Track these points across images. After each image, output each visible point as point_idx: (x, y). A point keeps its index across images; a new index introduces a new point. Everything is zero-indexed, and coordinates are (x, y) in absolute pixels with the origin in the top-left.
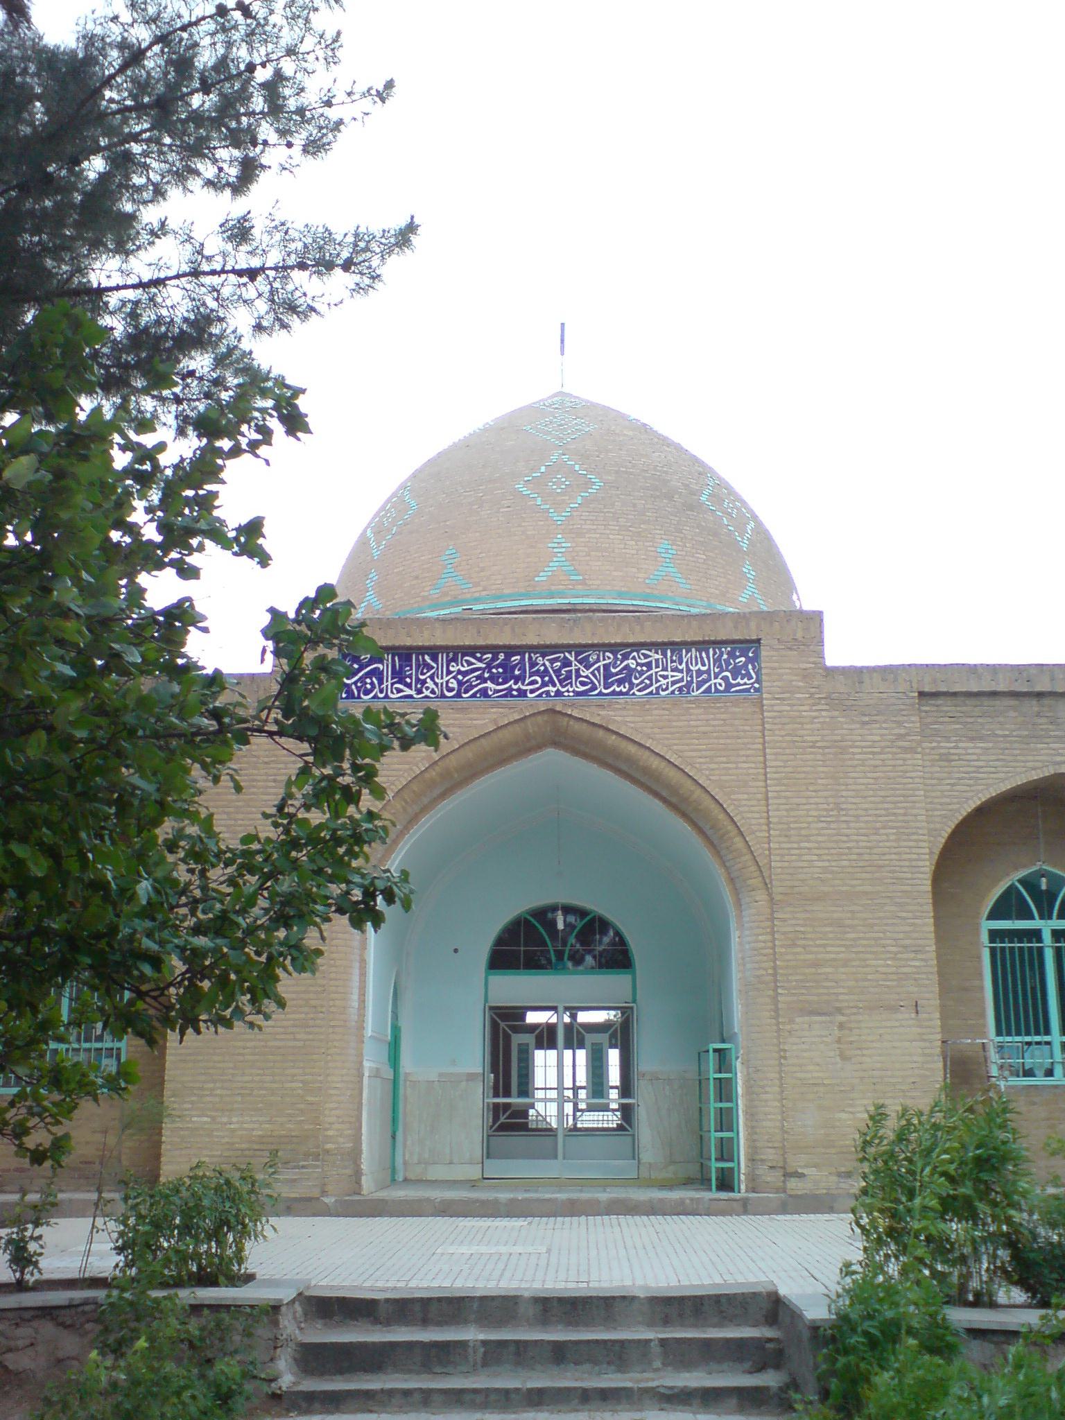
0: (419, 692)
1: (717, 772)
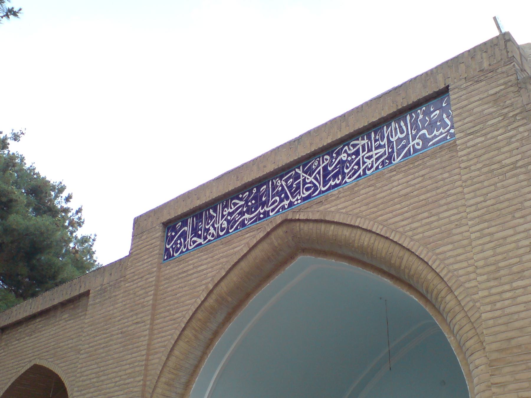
1: (420, 230)
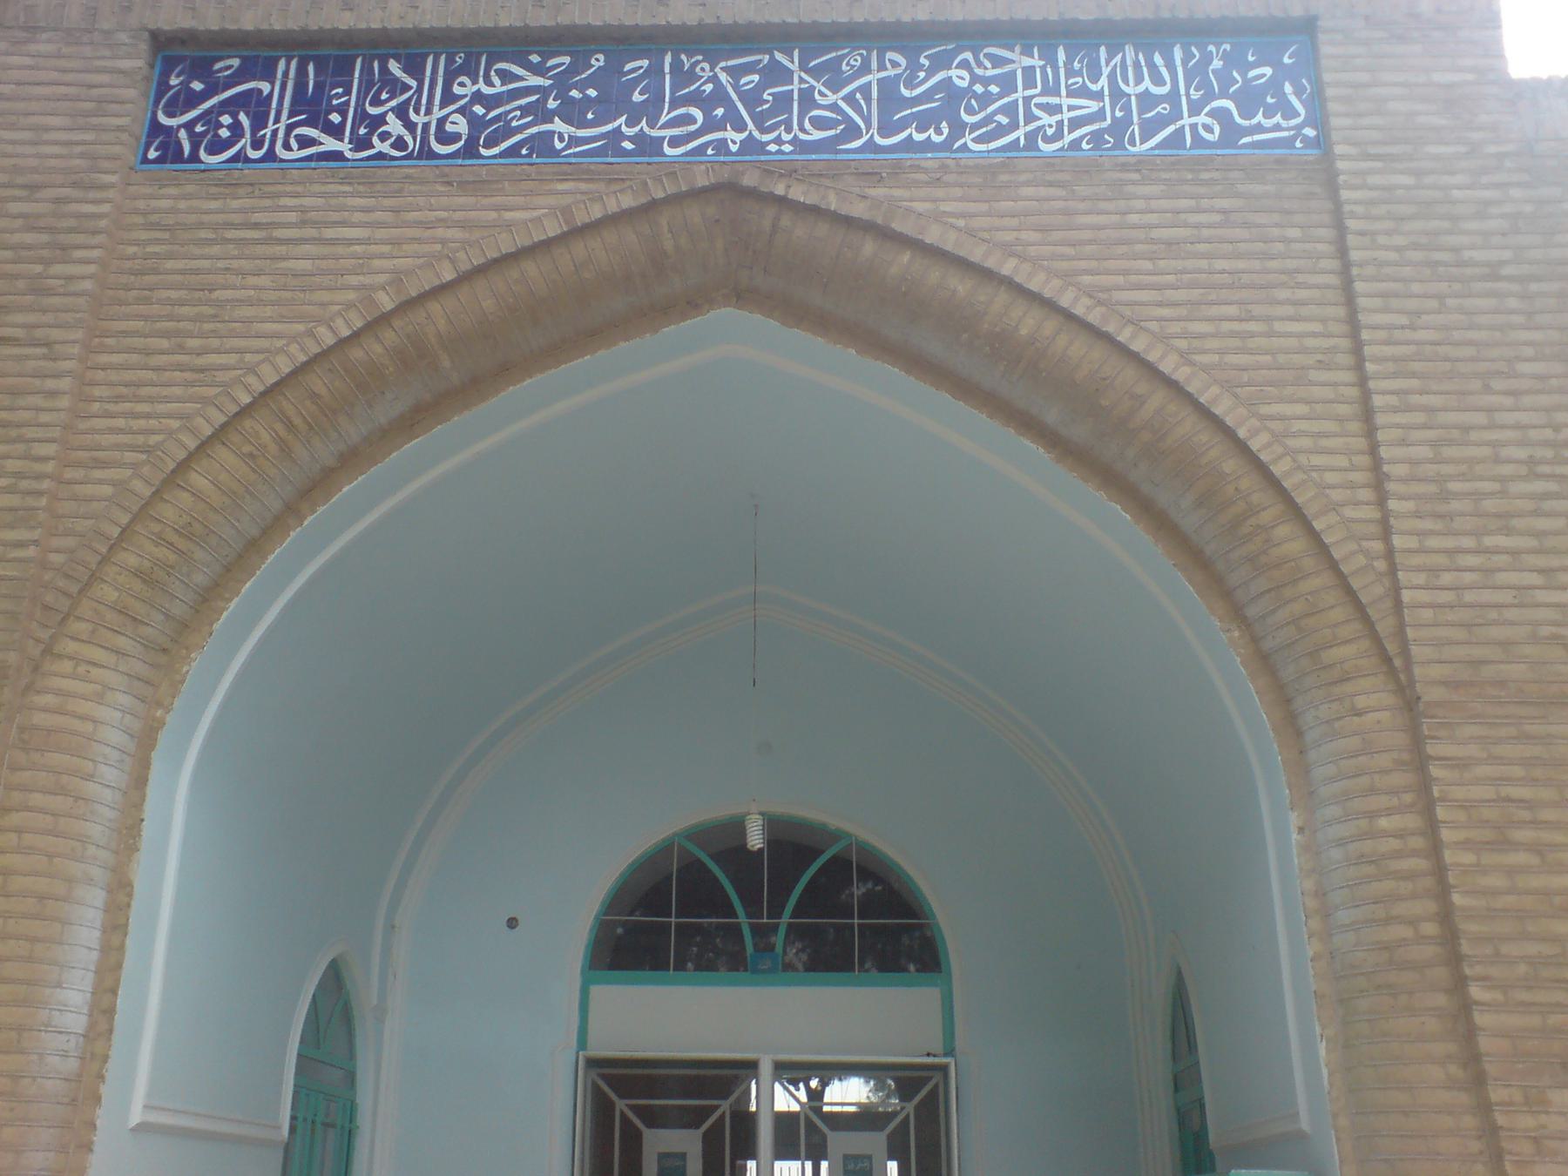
0: (361, 144)
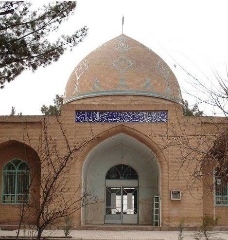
0: (93, 120)
